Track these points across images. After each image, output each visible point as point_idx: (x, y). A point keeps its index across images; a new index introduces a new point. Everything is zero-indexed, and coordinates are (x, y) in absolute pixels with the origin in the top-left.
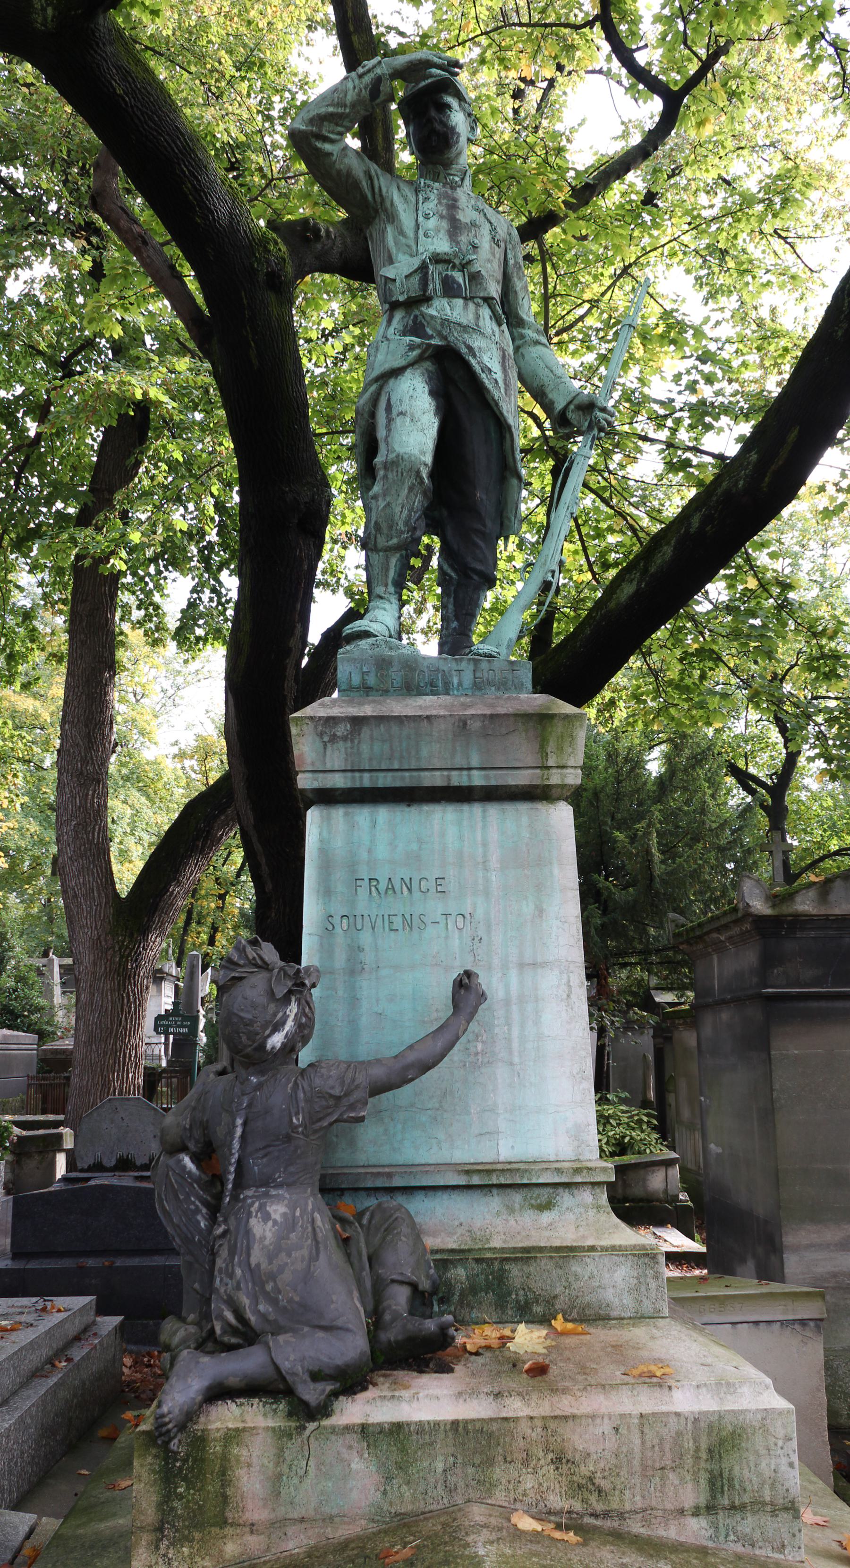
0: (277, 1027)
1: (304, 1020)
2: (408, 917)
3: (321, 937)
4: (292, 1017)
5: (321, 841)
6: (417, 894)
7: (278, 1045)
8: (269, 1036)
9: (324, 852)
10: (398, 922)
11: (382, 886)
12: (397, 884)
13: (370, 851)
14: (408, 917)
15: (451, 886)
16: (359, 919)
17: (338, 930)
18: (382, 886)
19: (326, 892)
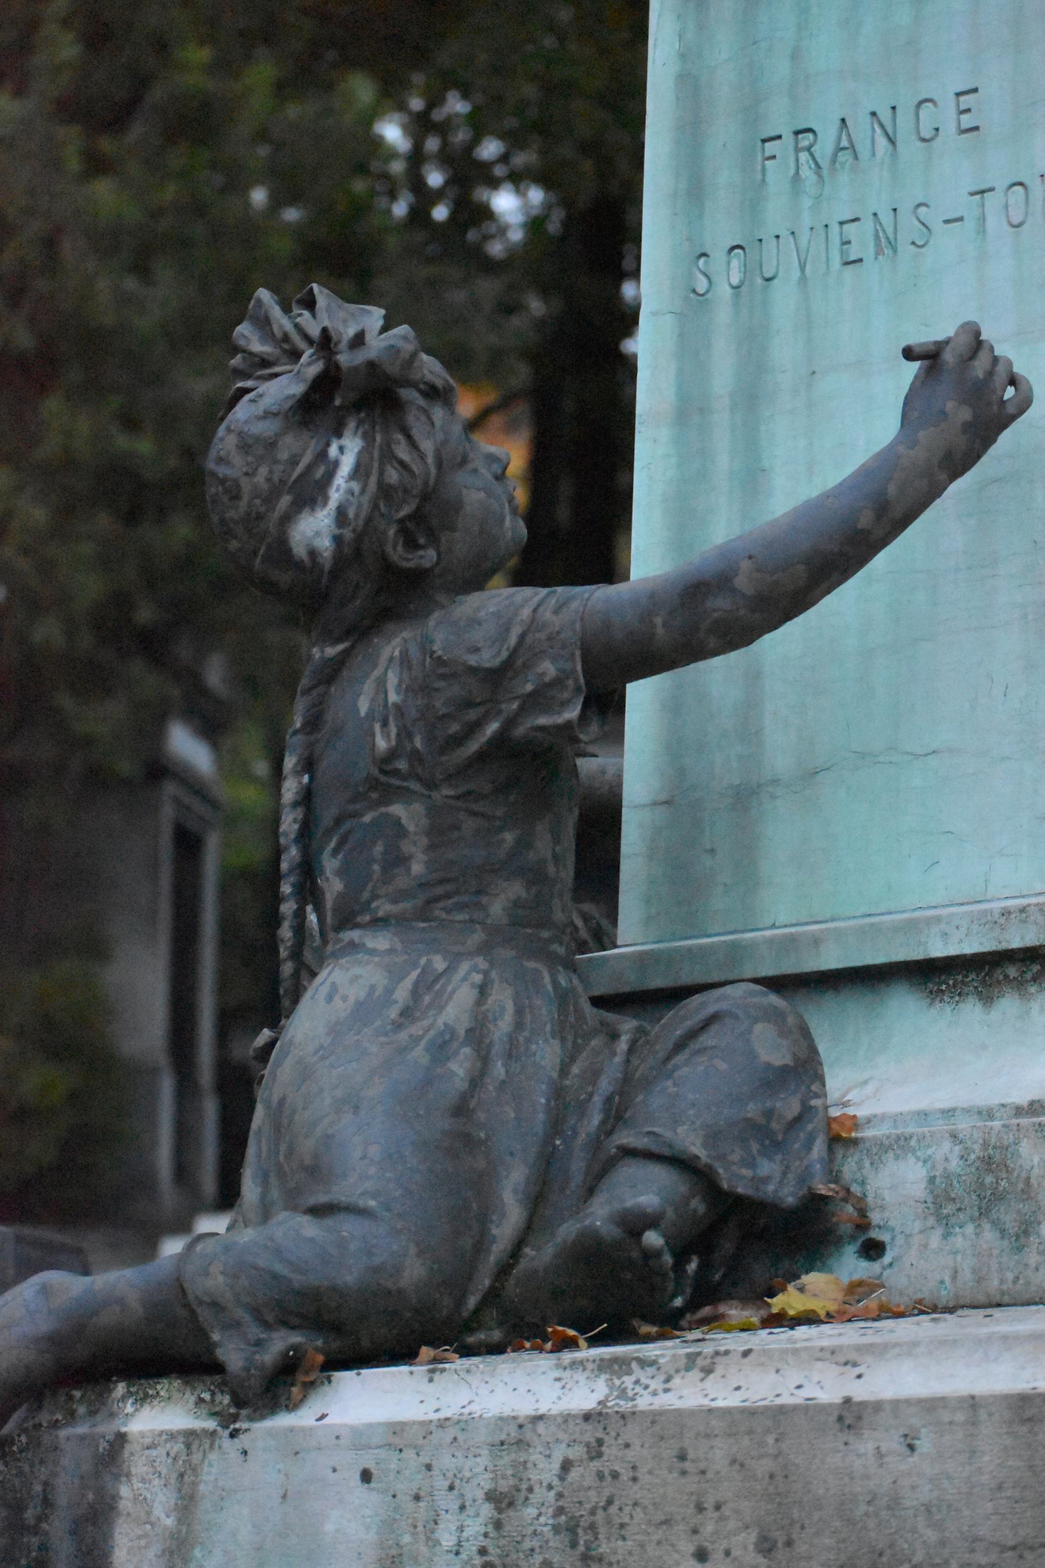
0: (310, 492)
1: (393, 476)
2: (886, 219)
3: (681, 316)
4: (347, 464)
5: (683, 57)
6: (909, 148)
7: (325, 544)
8: (288, 519)
9: (691, 85)
10: (861, 237)
11: (825, 147)
12: (861, 129)
13: (795, 56)
14: (886, 219)
15: (994, 108)
16: (771, 244)
17: (723, 291)
18: (825, 147)
19: (694, 191)
